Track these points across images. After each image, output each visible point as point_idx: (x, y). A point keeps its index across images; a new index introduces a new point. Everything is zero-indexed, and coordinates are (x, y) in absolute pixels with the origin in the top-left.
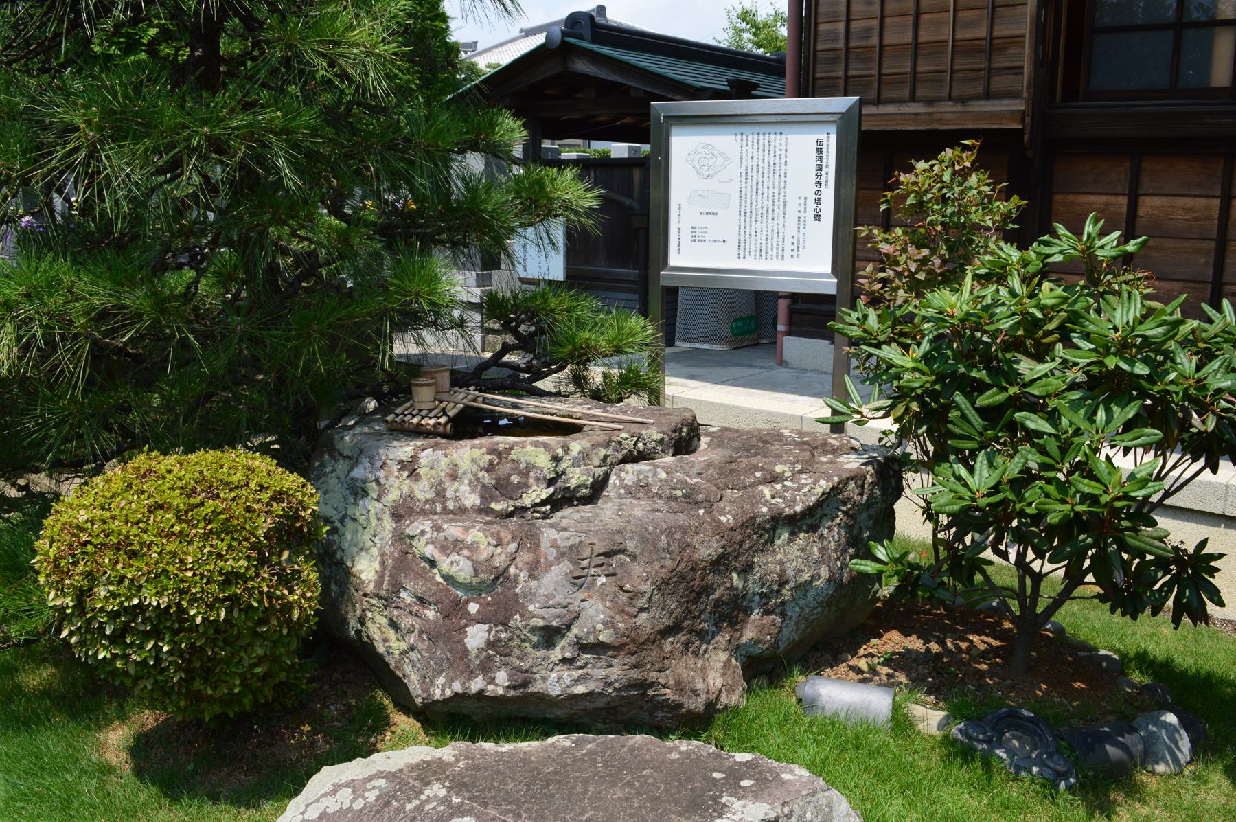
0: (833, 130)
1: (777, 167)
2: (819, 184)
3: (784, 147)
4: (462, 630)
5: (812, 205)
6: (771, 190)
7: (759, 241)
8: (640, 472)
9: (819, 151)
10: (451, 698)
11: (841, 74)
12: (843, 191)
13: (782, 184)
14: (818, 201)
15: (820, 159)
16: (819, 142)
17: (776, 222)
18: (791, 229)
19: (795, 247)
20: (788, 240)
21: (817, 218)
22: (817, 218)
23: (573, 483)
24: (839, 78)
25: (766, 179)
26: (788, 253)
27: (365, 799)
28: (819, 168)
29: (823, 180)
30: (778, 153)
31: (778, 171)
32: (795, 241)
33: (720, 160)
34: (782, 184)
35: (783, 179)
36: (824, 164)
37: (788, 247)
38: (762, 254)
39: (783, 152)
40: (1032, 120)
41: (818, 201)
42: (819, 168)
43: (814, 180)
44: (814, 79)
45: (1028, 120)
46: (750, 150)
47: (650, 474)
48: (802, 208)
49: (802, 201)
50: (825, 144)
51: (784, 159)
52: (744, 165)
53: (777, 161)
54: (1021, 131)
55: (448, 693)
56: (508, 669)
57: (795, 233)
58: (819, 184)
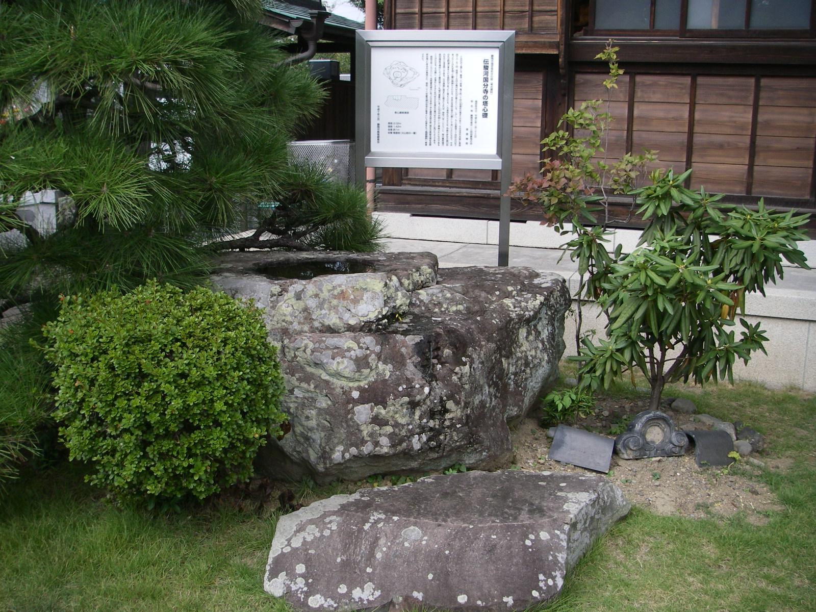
0: (496, 53)
1: (454, 79)
2: (486, 91)
3: (459, 65)
4: (351, 411)
5: (481, 106)
6: (450, 96)
7: (441, 133)
8: (433, 295)
9: (486, 68)
10: (349, 460)
11: (417, 10)
12: (505, 97)
13: (459, 91)
14: (485, 103)
15: (487, 73)
16: (486, 61)
17: (454, 118)
18: (466, 123)
19: (469, 137)
20: (464, 132)
21: (485, 115)
22: (485, 115)
23: (398, 303)
24: (415, 13)
25: (446, 88)
26: (463, 141)
27: (330, 529)
28: (486, 80)
29: (489, 89)
30: (455, 69)
31: (455, 82)
32: (469, 132)
33: (410, 74)
34: (459, 91)
35: (459, 87)
36: (489, 77)
37: (464, 136)
38: (444, 141)
39: (459, 69)
40: (565, 47)
41: (485, 103)
42: (486, 80)
43: (482, 88)
44: (395, 14)
45: (562, 47)
46: (434, 66)
47: (440, 295)
48: (474, 109)
49: (474, 104)
50: (490, 63)
51: (459, 73)
52: (429, 77)
53: (455, 74)
54: (557, 56)
55: (347, 456)
56: (650, 390)
57: (468, 126)
58: (486, 91)
